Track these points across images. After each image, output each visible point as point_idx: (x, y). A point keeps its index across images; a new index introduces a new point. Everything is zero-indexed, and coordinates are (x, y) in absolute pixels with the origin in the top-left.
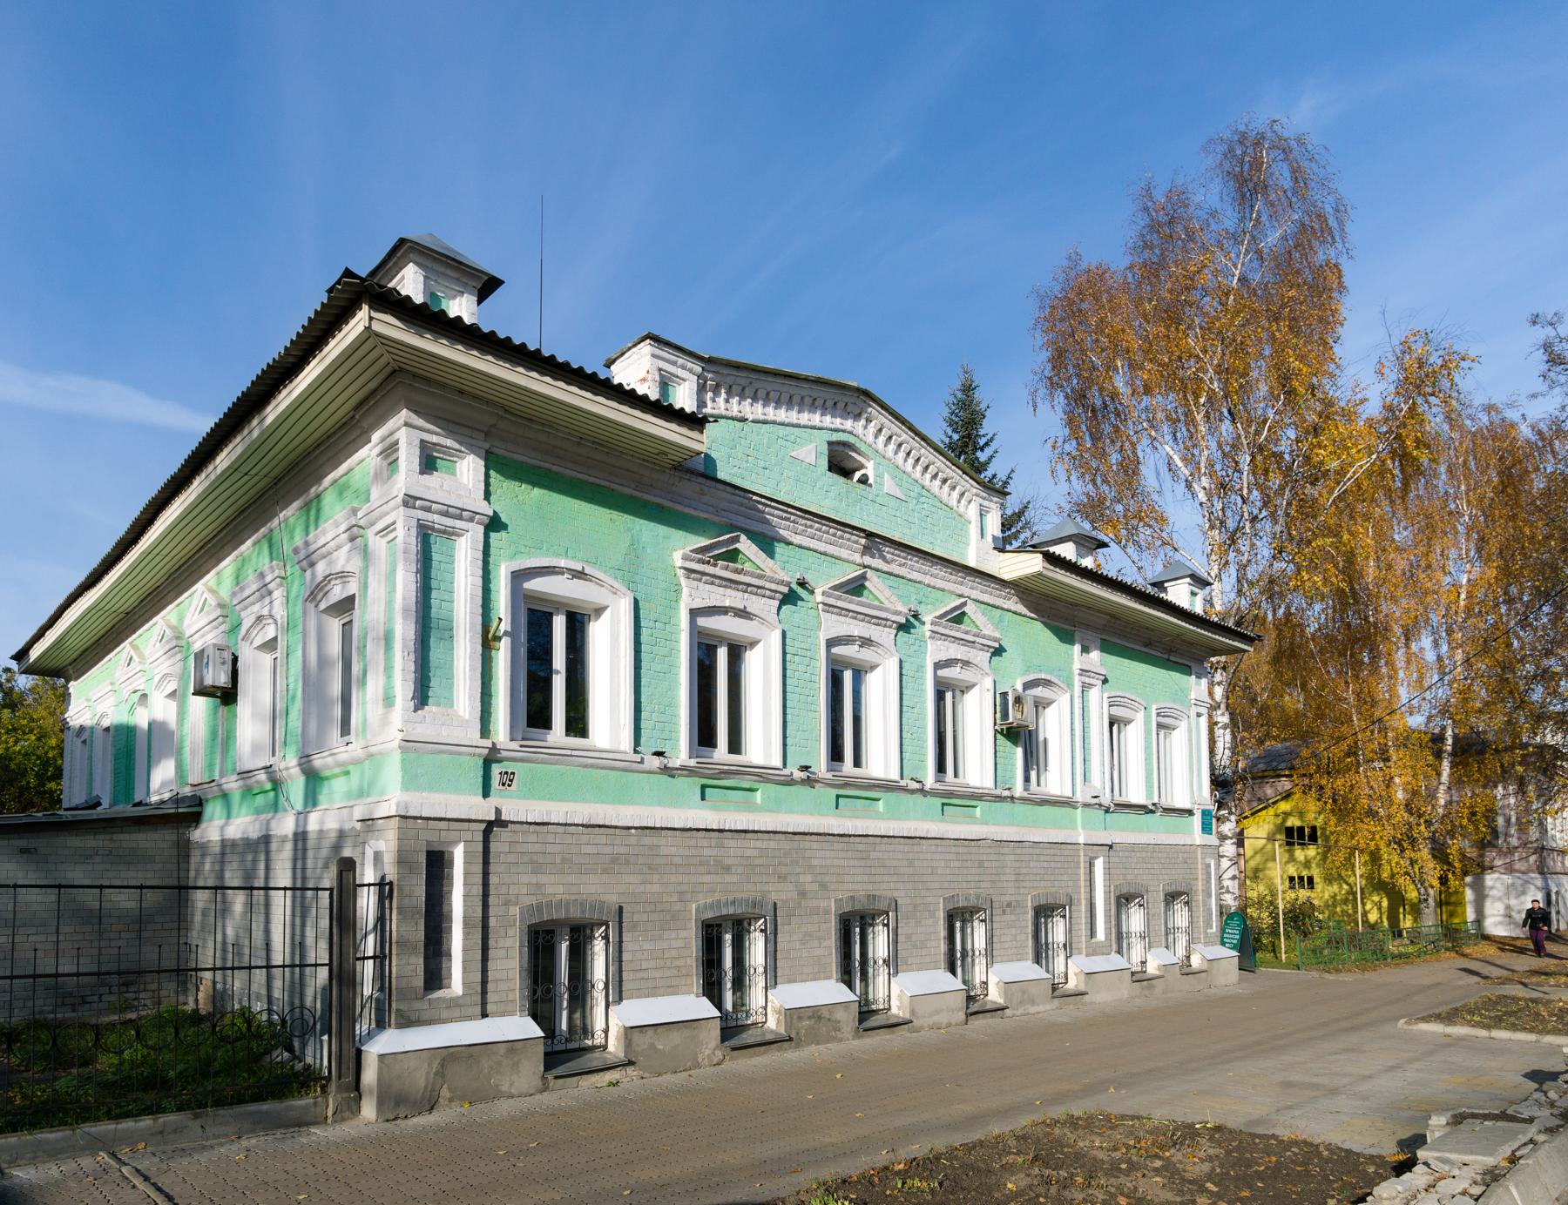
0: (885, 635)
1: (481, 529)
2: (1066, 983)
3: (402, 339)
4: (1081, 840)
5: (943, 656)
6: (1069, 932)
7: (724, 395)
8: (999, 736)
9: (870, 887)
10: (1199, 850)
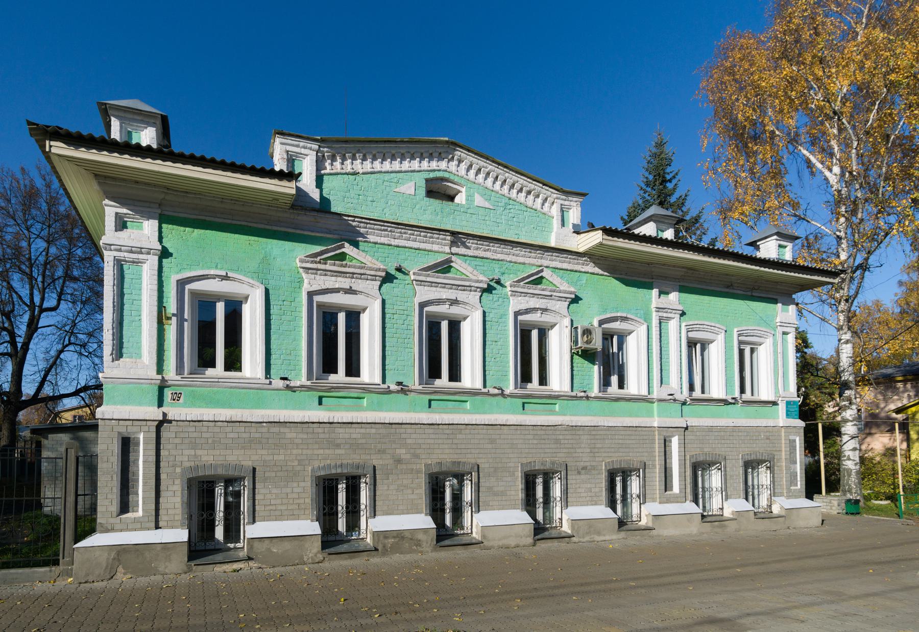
0: (474, 297)
1: (156, 258)
2: (640, 521)
3: (116, 163)
4: (656, 425)
5: (523, 307)
6: (644, 486)
7: (339, 160)
8: (575, 357)
9: (456, 456)
10: (783, 430)
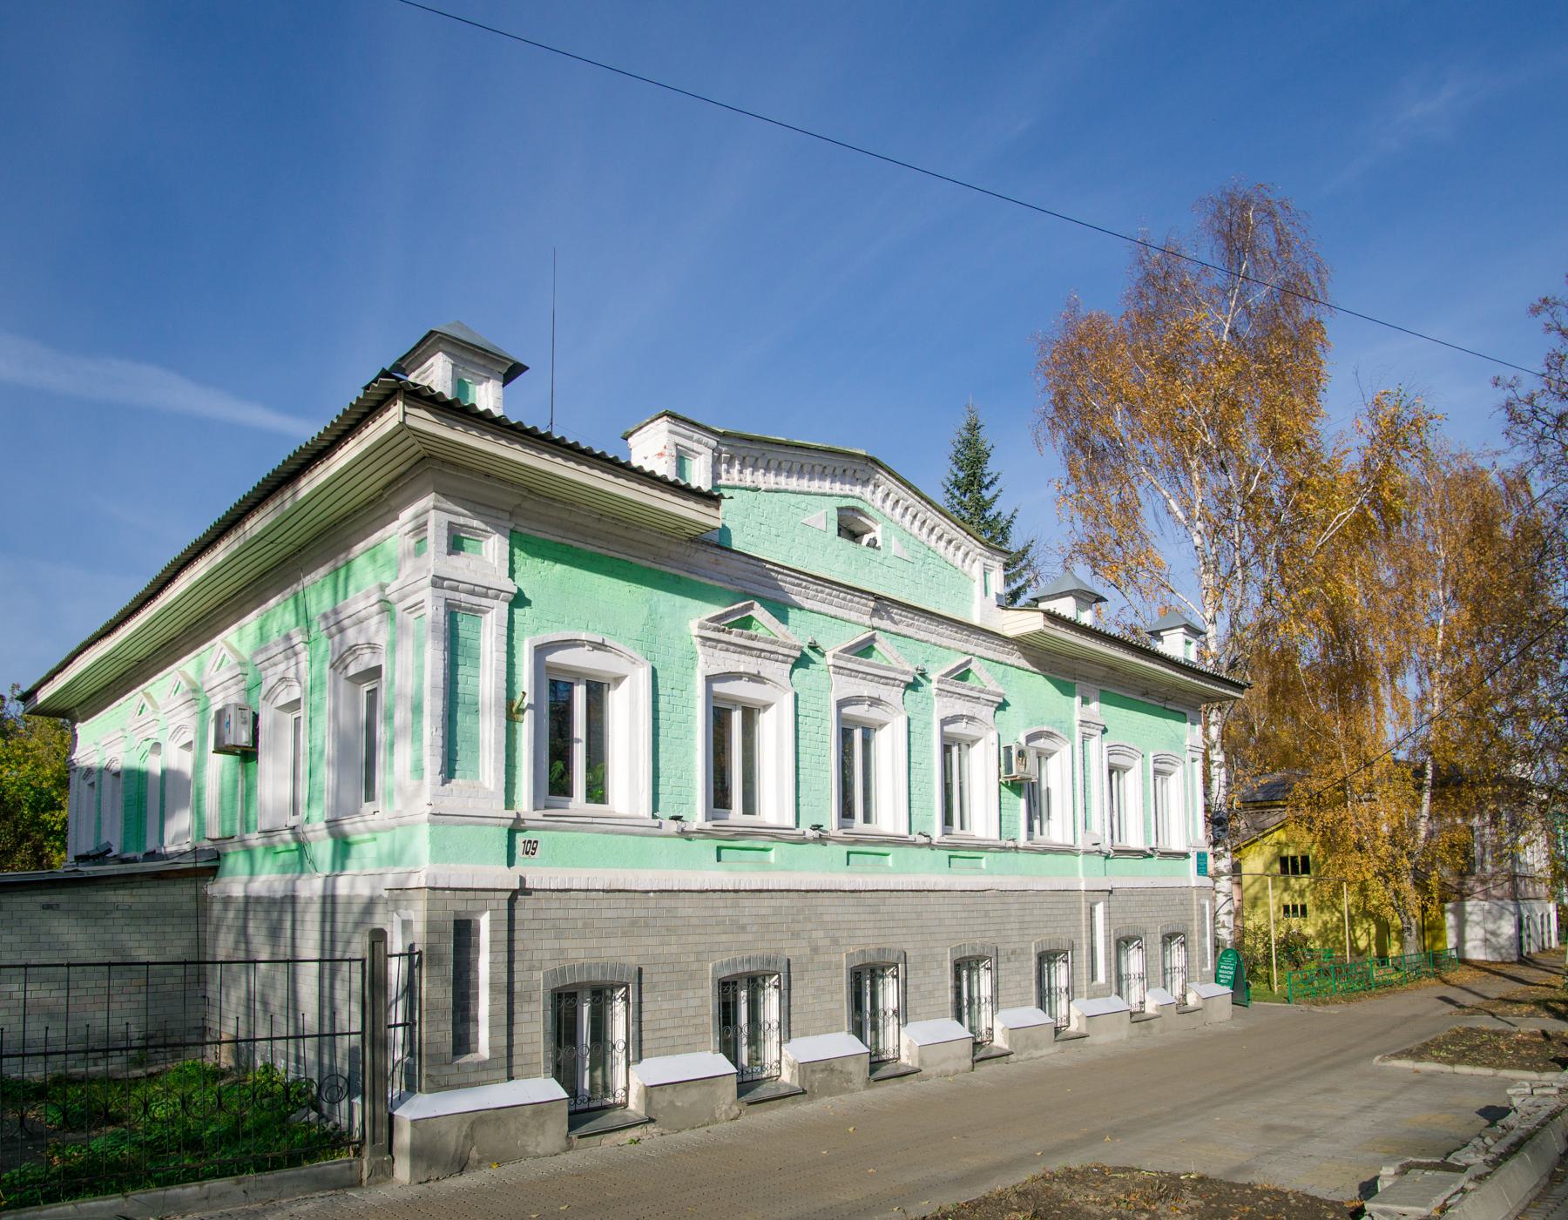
0: (892, 694)
1: (506, 606)
2: (1068, 1026)
5: (950, 713)
6: (1071, 976)
7: (737, 467)
8: (1003, 788)
9: (881, 940)
10: (1195, 892)
